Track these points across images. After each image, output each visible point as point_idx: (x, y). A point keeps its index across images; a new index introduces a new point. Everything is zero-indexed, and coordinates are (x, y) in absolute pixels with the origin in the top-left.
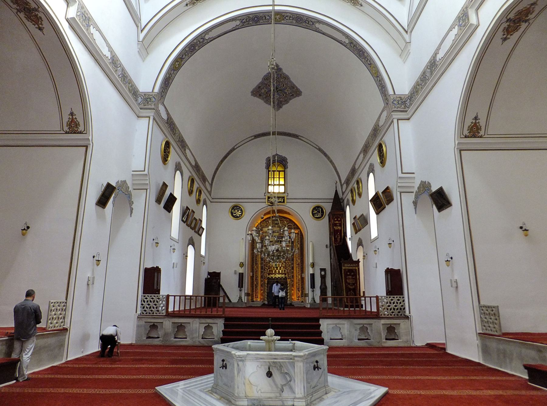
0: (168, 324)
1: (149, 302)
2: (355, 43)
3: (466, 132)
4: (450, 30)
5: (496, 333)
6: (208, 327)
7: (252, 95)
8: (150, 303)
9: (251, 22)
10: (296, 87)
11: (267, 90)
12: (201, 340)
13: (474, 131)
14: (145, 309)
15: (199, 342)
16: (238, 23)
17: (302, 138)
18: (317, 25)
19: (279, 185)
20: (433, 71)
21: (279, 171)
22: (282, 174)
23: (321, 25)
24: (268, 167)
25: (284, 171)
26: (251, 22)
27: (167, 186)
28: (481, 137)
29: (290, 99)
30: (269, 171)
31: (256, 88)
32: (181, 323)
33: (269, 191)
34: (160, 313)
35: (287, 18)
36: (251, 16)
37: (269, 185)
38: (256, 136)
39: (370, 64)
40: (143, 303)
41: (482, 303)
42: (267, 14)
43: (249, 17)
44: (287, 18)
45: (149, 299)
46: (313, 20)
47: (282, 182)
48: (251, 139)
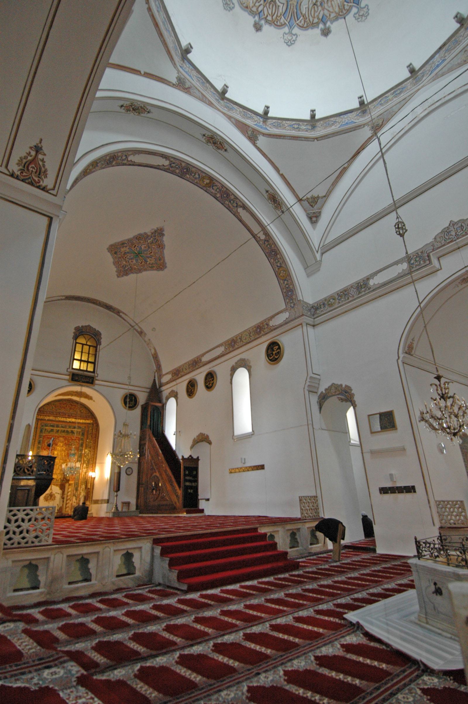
0: (59, 559)
1: (20, 522)
2: (271, 242)
3: (407, 349)
4: (396, 263)
5: (462, 526)
6: (128, 556)
7: (107, 249)
8: (22, 524)
9: (177, 171)
10: (164, 261)
11: (128, 251)
12: (115, 579)
13: (409, 350)
14: (11, 535)
15: (113, 583)
16: (167, 163)
17: (123, 316)
18: (240, 210)
19: (88, 362)
20: (360, 291)
21: (90, 346)
22: (92, 350)
23: (245, 211)
24: (76, 337)
25: (96, 347)
26: (177, 171)
27: (77, 329)
28: (412, 355)
29: (146, 270)
30: (76, 343)
31: (118, 243)
32: (82, 554)
33: (74, 367)
34: (40, 541)
36: (183, 164)
37: (74, 359)
38: (69, 298)
39: (281, 267)
40: (8, 524)
41: (436, 499)
42: (200, 173)
43: (181, 164)
45: (21, 515)
46: (239, 203)
47: (91, 359)
48: (59, 298)
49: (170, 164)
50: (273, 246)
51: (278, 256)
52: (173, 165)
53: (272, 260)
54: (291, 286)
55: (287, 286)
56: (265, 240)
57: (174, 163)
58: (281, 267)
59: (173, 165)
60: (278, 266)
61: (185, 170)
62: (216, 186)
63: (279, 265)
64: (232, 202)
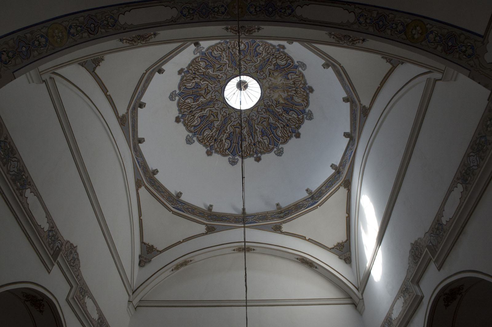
35: (223, 9)
44: (223, 9)
49: (293, 11)
50: (103, 30)
51: (85, 35)
52: (290, 11)
53: (81, 19)
54: (36, 53)
55: (36, 43)
56: (116, 21)
57: (290, 14)
58: (69, 33)
59: (290, 11)
60: (71, 27)
61: (271, 9)
62: (223, 13)
63: (72, 31)
64: (191, 12)
